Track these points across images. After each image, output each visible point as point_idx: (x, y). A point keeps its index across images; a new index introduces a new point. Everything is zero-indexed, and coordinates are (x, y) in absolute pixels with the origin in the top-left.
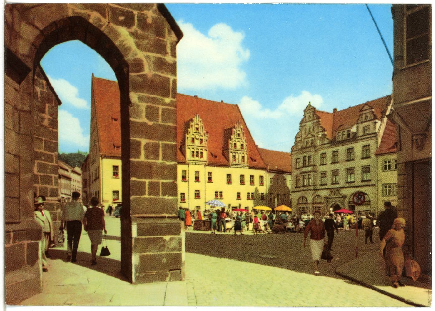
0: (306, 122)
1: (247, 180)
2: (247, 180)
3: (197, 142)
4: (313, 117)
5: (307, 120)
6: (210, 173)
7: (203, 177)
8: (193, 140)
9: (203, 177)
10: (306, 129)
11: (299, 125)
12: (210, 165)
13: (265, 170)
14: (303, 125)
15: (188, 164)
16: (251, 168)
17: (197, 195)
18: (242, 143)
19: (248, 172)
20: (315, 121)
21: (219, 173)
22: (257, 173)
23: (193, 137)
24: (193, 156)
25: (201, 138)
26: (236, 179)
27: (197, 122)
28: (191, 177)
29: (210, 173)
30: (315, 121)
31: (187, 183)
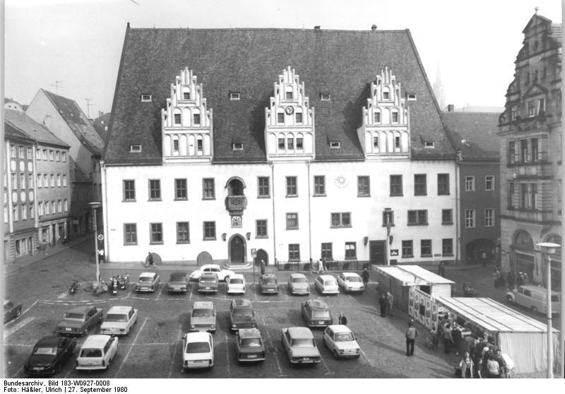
0: (528, 57)
1: (408, 184)
2: (408, 184)
3: (290, 120)
4: (544, 46)
5: (532, 52)
6: (320, 180)
7: (305, 186)
8: (281, 117)
9: (305, 186)
10: (529, 74)
11: (514, 66)
12: (320, 158)
13: (452, 161)
14: (522, 64)
15: (271, 163)
16: (415, 157)
17: (293, 221)
18: (396, 111)
19: (409, 171)
20: (548, 54)
21: (341, 174)
22: (432, 171)
23: (282, 111)
24: (282, 146)
25: (298, 110)
26: (380, 186)
27: (288, 82)
28: (279, 186)
29: (320, 180)
30: (548, 54)
31: (271, 200)
